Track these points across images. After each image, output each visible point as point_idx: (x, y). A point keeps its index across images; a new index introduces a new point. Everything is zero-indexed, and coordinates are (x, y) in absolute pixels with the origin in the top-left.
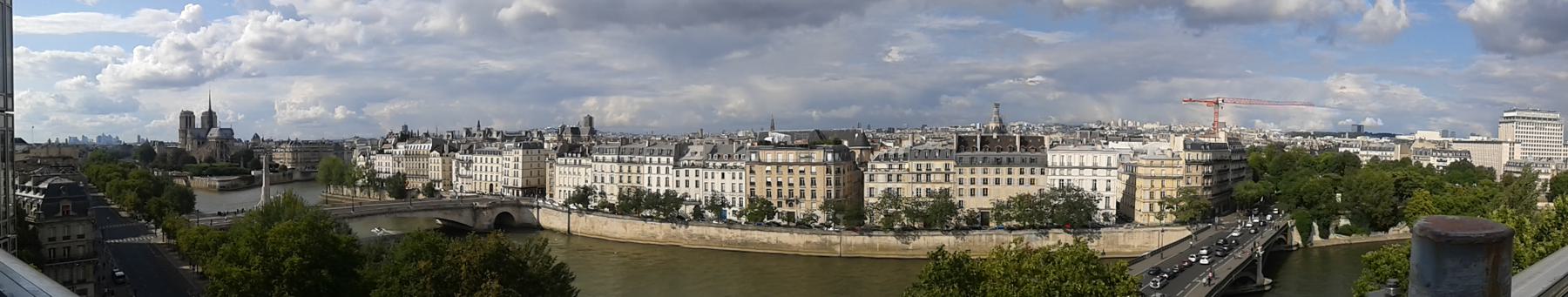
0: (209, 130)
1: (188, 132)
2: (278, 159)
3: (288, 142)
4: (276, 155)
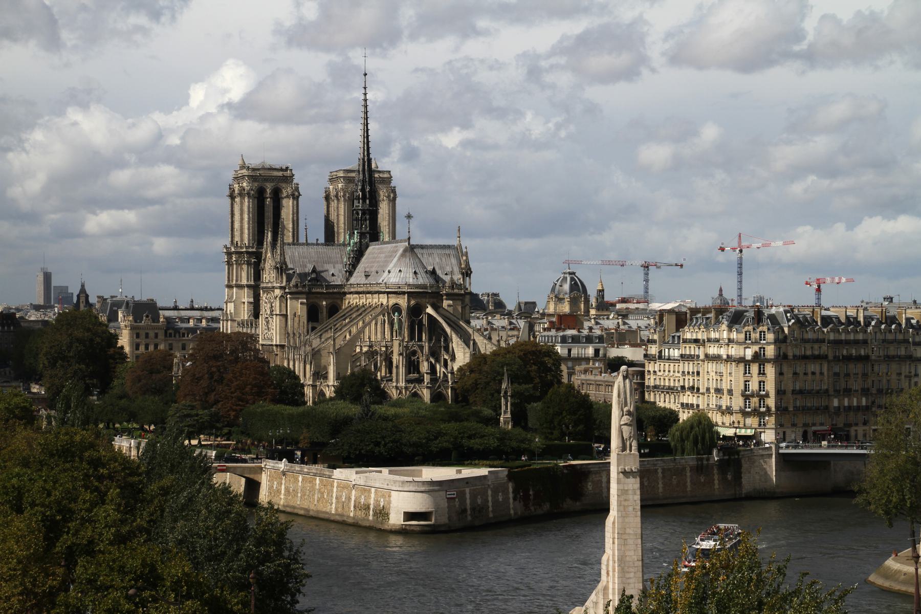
0: (359, 254)
1: (269, 264)
2: (670, 390)
3: (720, 311)
4: (657, 374)
